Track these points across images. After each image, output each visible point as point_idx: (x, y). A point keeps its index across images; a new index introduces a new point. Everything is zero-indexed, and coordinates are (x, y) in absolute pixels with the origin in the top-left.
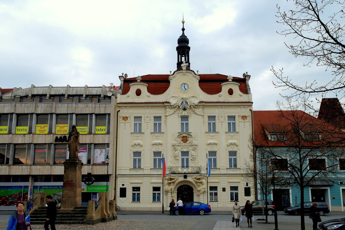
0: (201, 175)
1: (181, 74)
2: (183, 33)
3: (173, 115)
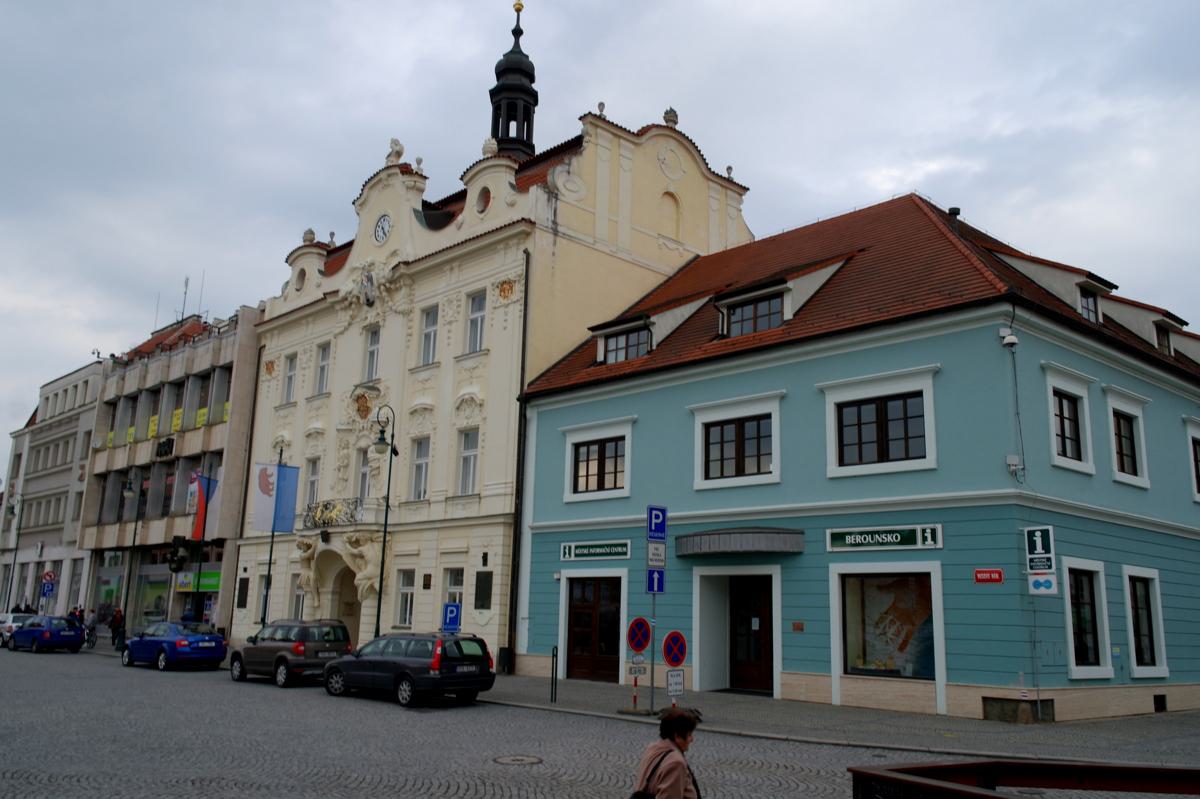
0: (359, 528)
1: (380, 186)
2: (517, 44)
3: (351, 328)
